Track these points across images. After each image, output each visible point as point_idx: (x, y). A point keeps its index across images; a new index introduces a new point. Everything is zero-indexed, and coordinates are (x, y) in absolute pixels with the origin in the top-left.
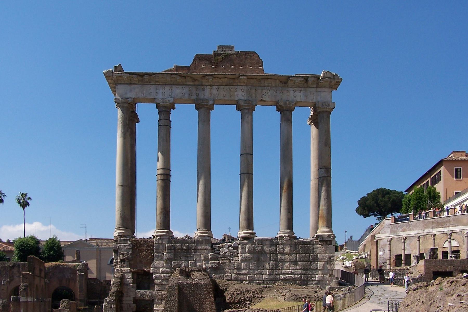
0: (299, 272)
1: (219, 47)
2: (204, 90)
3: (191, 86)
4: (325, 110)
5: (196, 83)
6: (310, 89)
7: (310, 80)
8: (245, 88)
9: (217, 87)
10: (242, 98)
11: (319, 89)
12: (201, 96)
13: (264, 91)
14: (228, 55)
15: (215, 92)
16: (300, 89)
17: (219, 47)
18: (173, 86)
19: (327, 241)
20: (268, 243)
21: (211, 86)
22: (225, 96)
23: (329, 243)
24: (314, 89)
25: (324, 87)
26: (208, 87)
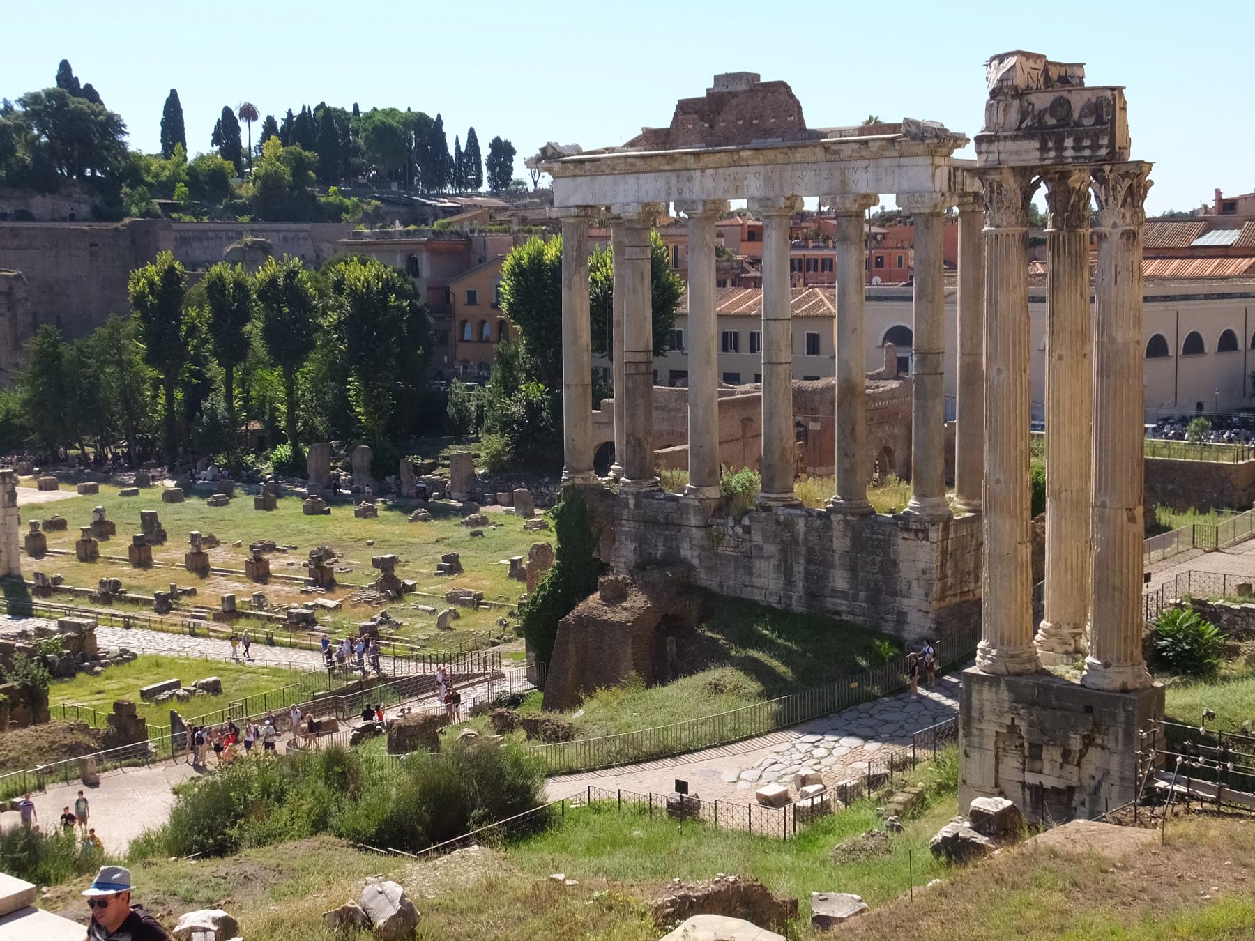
0: (862, 594)
1: (717, 78)
2: (690, 179)
3: (668, 174)
4: (916, 211)
5: (678, 165)
6: (886, 162)
7: (874, 147)
8: (761, 169)
9: (712, 171)
10: (757, 194)
11: (904, 161)
12: (686, 195)
13: (798, 173)
14: (734, 95)
15: (709, 183)
16: (866, 163)
17: (717, 78)
18: (642, 176)
19: (917, 532)
20: (801, 522)
21: (703, 170)
22: (726, 191)
23: (920, 535)
24: (895, 162)
25: (916, 155)
26: (698, 173)
